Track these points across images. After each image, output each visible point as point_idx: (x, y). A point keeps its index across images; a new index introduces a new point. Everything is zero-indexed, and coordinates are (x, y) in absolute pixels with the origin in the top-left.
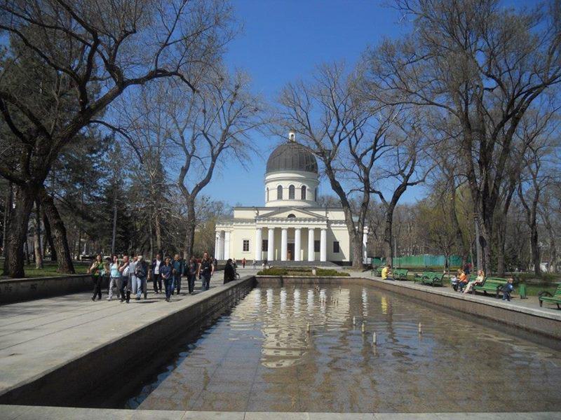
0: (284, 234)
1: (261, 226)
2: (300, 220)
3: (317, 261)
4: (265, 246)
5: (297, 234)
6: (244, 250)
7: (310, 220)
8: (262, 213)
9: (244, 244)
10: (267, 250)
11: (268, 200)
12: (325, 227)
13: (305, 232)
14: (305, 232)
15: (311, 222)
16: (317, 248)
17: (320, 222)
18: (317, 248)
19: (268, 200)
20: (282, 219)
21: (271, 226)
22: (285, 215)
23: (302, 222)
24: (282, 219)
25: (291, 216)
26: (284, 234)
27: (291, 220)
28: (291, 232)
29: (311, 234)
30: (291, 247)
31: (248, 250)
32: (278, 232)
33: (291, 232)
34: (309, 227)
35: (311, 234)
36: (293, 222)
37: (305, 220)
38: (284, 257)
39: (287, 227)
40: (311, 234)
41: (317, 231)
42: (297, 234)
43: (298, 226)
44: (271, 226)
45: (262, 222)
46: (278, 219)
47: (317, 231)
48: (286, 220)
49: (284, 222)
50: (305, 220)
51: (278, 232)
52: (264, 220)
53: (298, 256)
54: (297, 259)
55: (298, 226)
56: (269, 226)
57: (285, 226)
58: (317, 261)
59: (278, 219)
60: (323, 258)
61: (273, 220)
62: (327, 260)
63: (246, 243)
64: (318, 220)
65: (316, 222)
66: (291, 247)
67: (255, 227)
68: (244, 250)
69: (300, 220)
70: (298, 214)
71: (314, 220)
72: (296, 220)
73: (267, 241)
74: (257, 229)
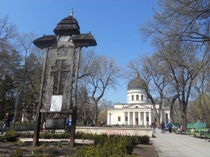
0: (134, 114)
1: (125, 111)
2: (140, 108)
5: (139, 114)
6: (119, 121)
7: (144, 108)
8: (125, 106)
9: (119, 118)
10: (127, 121)
12: (151, 111)
13: (142, 113)
14: (142, 113)
15: (145, 109)
17: (148, 109)
20: (133, 109)
21: (129, 111)
22: (134, 107)
23: (141, 109)
24: (133, 109)
26: (134, 114)
27: (137, 109)
28: (137, 113)
30: (137, 120)
31: (120, 121)
32: (131, 113)
33: (137, 113)
35: (145, 114)
36: (137, 109)
37: (142, 108)
39: (135, 111)
41: (147, 113)
42: (139, 114)
43: (139, 111)
44: (129, 111)
45: (125, 109)
46: (131, 108)
47: (147, 113)
48: (135, 109)
49: (134, 109)
50: (142, 108)
51: (131, 113)
52: (126, 109)
54: (139, 124)
55: (139, 111)
57: (134, 111)
59: (131, 108)
61: (129, 109)
63: (119, 118)
64: (148, 109)
65: (147, 109)
66: (137, 120)
67: (122, 112)
68: (119, 121)
69: (140, 108)
70: (139, 106)
71: (146, 109)
72: (138, 109)
73: (127, 117)
74: (123, 112)
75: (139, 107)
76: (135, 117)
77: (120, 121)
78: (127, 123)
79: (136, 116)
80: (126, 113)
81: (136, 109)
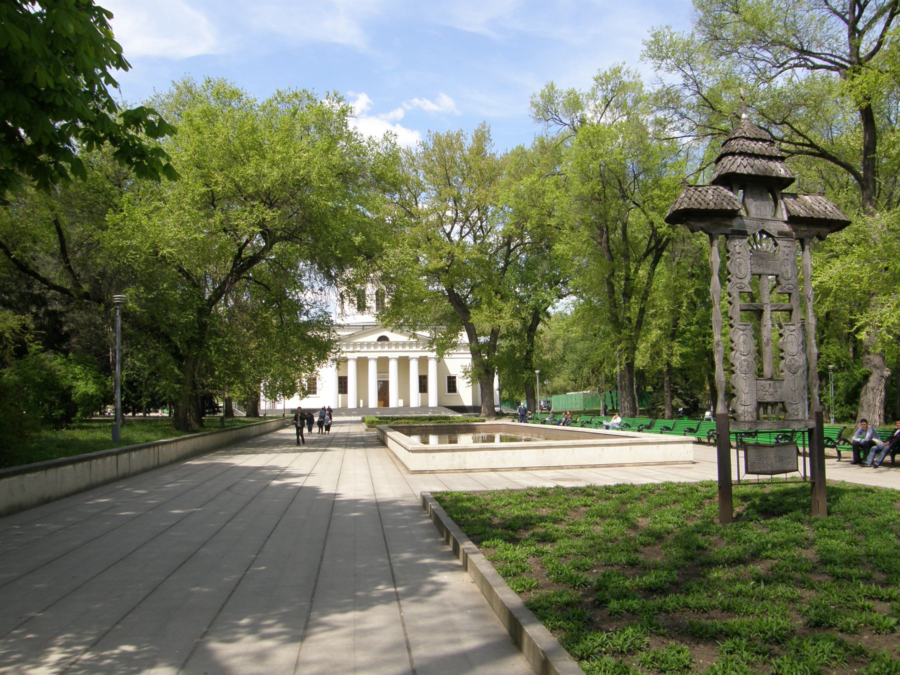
0: (372, 367)
3: (424, 406)
5: (393, 367)
13: (404, 363)
14: (404, 363)
16: (423, 387)
18: (423, 387)
20: (369, 344)
22: (374, 338)
25: (383, 339)
26: (372, 367)
27: (383, 346)
28: (383, 363)
29: (414, 367)
33: (383, 363)
34: (410, 355)
36: (386, 349)
38: (373, 402)
39: (377, 355)
40: (414, 367)
42: (393, 367)
48: (375, 345)
49: (372, 349)
50: (404, 344)
53: (395, 401)
55: (393, 354)
57: (373, 355)
58: (424, 406)
59: (362, 345)
60: (433, 402)
62: (439, 405)
69: (397, 344)
72: (390, 345)
75: (391, 340)
76: (378, 377)
78: (345, 402)
81: (379, 349)
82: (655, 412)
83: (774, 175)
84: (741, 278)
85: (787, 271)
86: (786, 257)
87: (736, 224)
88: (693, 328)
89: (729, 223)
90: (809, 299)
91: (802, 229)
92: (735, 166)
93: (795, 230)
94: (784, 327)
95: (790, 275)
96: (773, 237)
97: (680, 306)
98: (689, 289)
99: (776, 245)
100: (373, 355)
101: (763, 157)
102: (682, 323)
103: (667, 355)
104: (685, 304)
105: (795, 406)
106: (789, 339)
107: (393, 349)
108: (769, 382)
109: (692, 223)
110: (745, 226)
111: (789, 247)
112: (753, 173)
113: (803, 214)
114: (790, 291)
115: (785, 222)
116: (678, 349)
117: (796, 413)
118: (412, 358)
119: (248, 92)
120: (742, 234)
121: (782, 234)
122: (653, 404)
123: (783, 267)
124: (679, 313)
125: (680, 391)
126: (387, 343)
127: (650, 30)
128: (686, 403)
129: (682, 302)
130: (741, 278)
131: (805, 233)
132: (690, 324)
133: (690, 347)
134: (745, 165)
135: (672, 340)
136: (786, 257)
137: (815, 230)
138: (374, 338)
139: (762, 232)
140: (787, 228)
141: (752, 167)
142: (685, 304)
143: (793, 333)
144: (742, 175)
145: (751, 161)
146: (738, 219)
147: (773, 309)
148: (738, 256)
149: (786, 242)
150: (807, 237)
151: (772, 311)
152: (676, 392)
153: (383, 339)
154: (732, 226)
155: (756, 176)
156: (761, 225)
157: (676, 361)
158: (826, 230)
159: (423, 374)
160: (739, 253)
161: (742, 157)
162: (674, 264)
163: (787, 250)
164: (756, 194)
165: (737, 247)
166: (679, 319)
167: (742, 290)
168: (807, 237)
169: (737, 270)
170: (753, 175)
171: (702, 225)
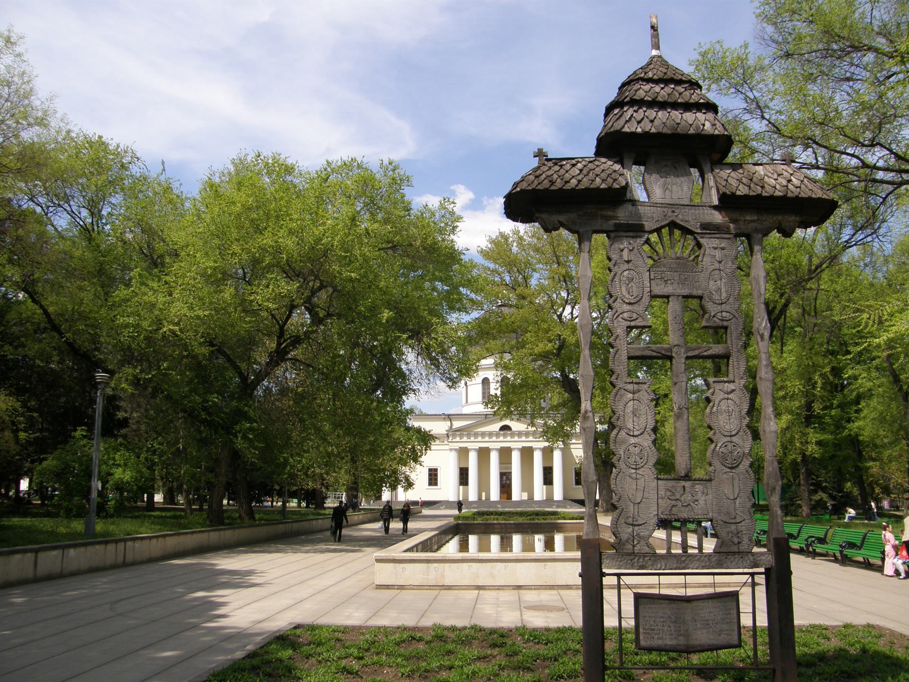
0: (494, 457)
1: (457, 446)
3: (549, 500)
4: (463, 477)
5: (516, 457)
6: (430, 484)
8: (457, 424)
11: (467, 402)
13: (527, 454)
14: (527, 454)
16: (548, 479)
18: (548, 479)
19: (467, 402)
20: (490, 434)
21: (473, 445)
22: (496, 427)
23: (523, 438)
25: (505, 428)
26: (494, 457)
27: (505, 436)
28: (505, 454)
29: (538, 457)
31: (436, 484)
32: (484, 454)
33: (505, 454)
36: (509, 439)
38: (495, 494)
40: (538, 457)
42: (516, 457)
43: (516, 444)
44: (473, 445)
48: (497, 435)
49: (494, 439)
50: (527, 434)
51: (484, 454)
52: (461, 436)
53: (517, 494)
55: (516, 444)
56: (469, 446)
57: (495, 445)
58: (549, 500)
59: (483, 434)
60: (558, 495)
62: (564, 499)
67: (447, 447)
68: (430, 484)
69: (520, 434)
72: (513, 435)
73: (467, 469)
74: (451, 450)
76: (500, 468)
77: (436, 484)
78: (466, 494)
79: (501, 463)
80: (463, 453)
81: (501, 439)
82: (793, 508)
83: (692, 131)
84: (630, 304)
85: (719, 289)
86: (717, 265)
87: (623, 214)
88: (833, 412)
89: (610, 213)
90: (762, 336)
91: (748, 218)
92: (621, 122)
93: (733, 221)
94: (712, 385)
95: (724, 295)
96: (691, 233)
97: (814, 388)
98: (823, 368)
99: (699, 246)
100: (495, 445)
101: (675, 106)
102: (817, 407)
103: (801, 443)
104: (819, 385)
105: (733, 527)
106: (723, 405)
107: (516, 438)
108: (683, 483)
109: (544, 216)
110: (640, 217)
111: (723, 249)
112: (653, 130)
113: (742, 191)
114: (725, 323)
115: (715, 208)
116: (814, 436)
117: (736, 540)
118: (536, 449)
119: (301, 165)
120: (635, 229)
121: (710, 228)
122: (791, 499)
123: (712, 283)
124: (814, 395)
125: (824, 484)
126: (509, 432)
127: (696, 47)
128: (833, 497)
129: (816, 383)
130: (630, 304)
131: (752, 225)
132: (831, 407)
133: (832, 433)
134: (639, 118)
135: (807, 427)
136: (717, 265)
137: (770, 219)
138: (496, 427)
139: (673, 225)
140: (718, 217)
141: (652, 121)
142: (819, 385)
143: (730, 396)
144: (633, 134)
145: (651, 113)
146: (629, 207)
147: (690, 354)
148: (626, 266)
149: (717, 241)
150: (757, 230)
151: (687, 358)
152: (820, 485)
153: (505, 428)
154: (616, 218)
155: (659, 136)
156: (670, 214)
157: (812, 449)
158: (793, 218)
159: (548, 465)
160: (628, 262)
161: (636, 108)
162: (807, 339)
163: (718, 254)
164: (666, 166)
165: (625, 253)
166: (813, 402)
167: (633, 324)
168: (757, 230)
169: (624, 289)
170: (653, 134)
171: (562, 218)
